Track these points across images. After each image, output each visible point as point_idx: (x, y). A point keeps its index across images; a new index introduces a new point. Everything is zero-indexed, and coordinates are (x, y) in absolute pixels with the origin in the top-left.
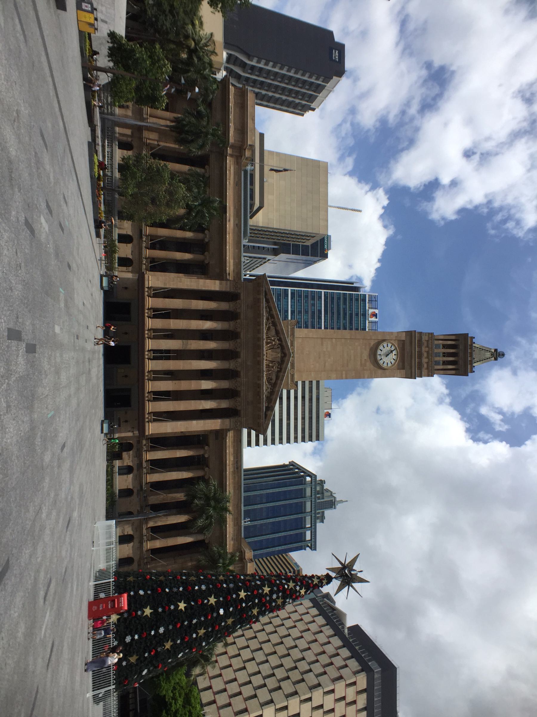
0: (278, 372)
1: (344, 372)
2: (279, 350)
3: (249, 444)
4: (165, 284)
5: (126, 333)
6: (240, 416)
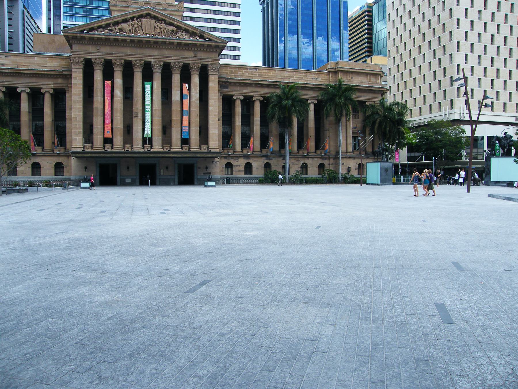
0: (166, 22)
2: (144, 20)
3: (235, 57)
4: (79, 133)
6: (208, 65)
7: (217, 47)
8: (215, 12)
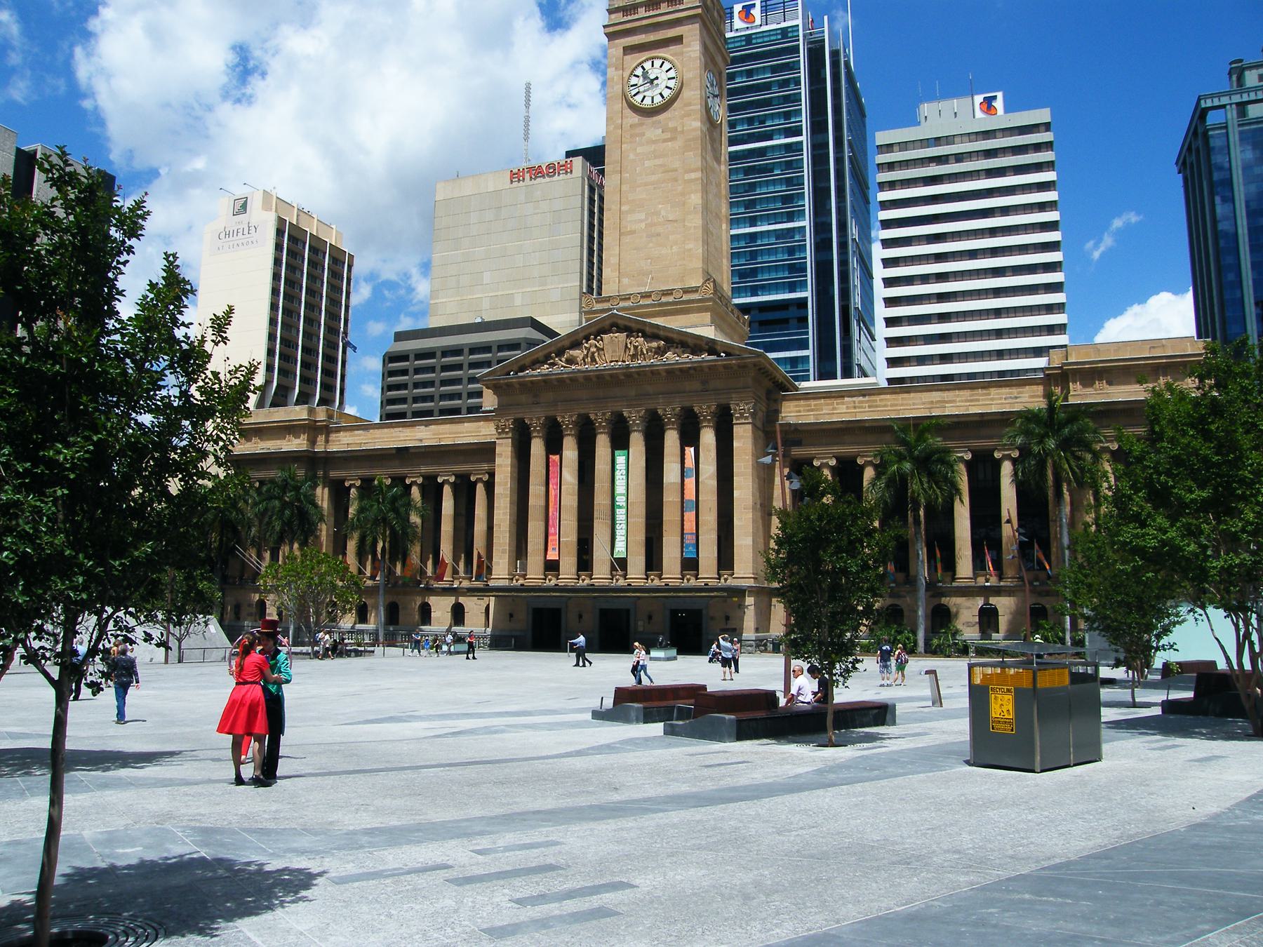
1: (687, 177)
5: (580, 616)
7: (743, 367)
8: (993, 232)
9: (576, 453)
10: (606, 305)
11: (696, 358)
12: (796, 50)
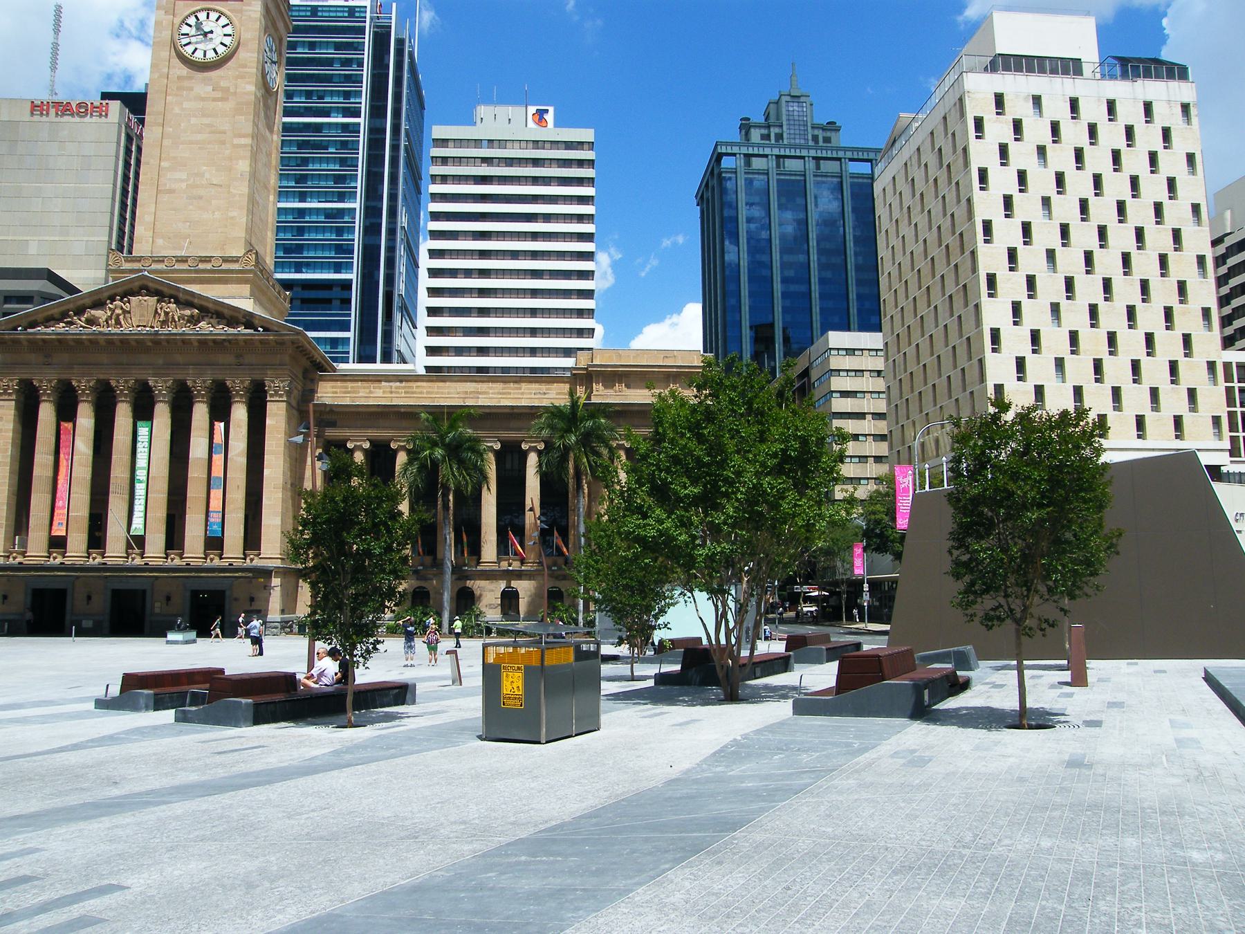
0: (177, 302)
1: (236, 141)
5: (89, 598)
7: (282, 343)
8: (535, 236)
9: (92, 421)
10: (136, 266)
11: (231, 331)
12: (361, 31)
